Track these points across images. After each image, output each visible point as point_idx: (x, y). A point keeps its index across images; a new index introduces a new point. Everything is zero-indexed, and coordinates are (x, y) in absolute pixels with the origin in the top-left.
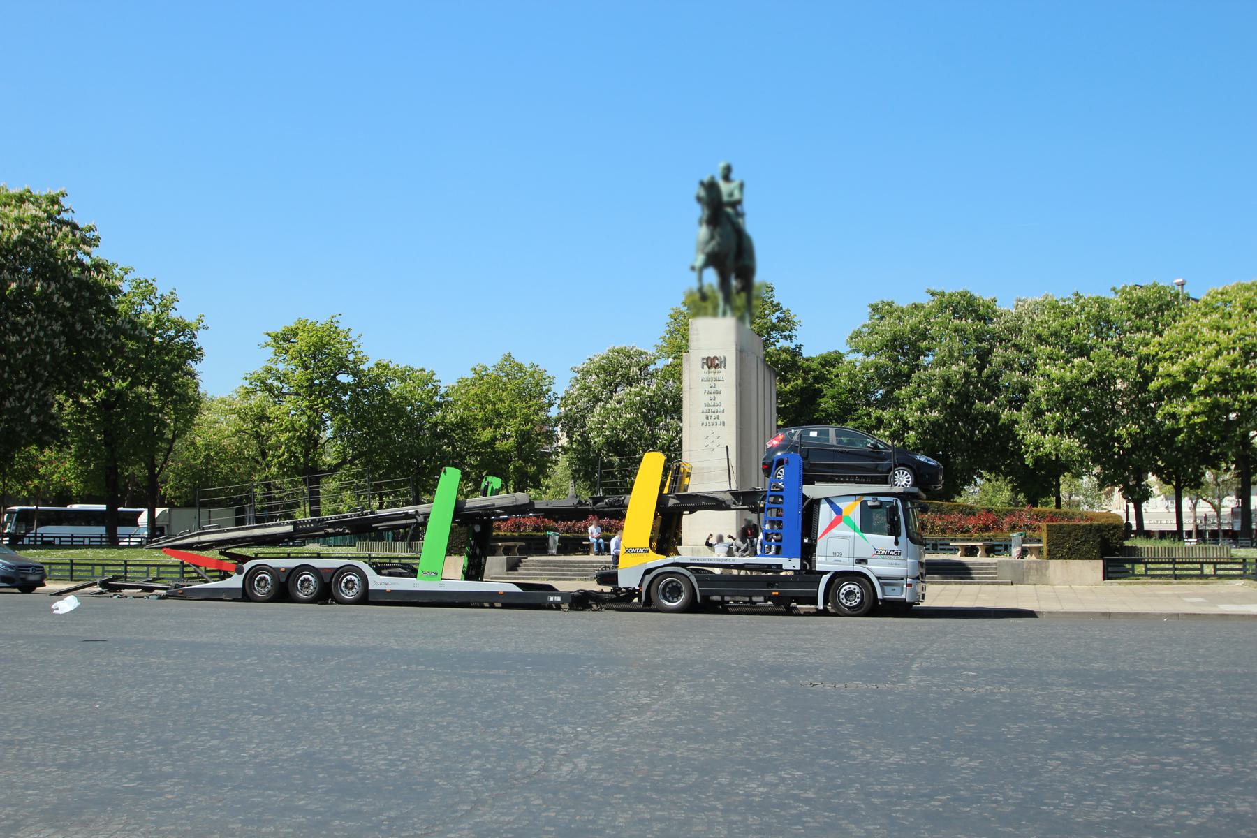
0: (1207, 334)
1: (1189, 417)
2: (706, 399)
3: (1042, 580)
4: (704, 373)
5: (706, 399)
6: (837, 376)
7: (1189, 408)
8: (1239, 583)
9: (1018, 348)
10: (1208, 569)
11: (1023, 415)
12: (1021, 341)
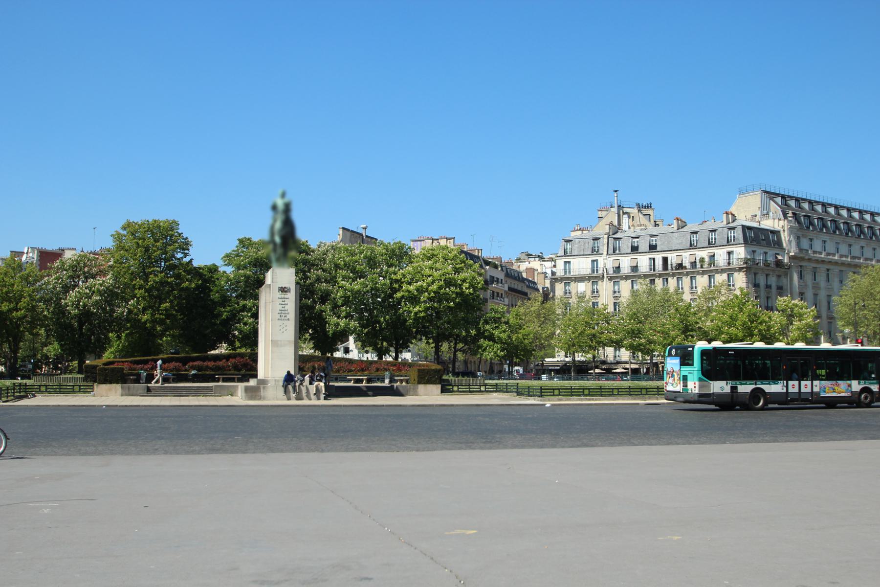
0: (427, 271)
1: (416, 313)
2: (280, 307)
3: (416, 394)
4: (279, 295)
5: (280, 307)
6: (218, 279)
7: (417, 309)
8: (495, 394)
9: (324, 270)
10: (483, 389)
11: (328, 307)
12: (326, 266)
